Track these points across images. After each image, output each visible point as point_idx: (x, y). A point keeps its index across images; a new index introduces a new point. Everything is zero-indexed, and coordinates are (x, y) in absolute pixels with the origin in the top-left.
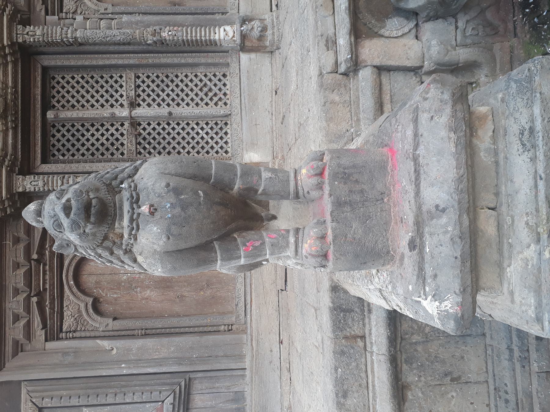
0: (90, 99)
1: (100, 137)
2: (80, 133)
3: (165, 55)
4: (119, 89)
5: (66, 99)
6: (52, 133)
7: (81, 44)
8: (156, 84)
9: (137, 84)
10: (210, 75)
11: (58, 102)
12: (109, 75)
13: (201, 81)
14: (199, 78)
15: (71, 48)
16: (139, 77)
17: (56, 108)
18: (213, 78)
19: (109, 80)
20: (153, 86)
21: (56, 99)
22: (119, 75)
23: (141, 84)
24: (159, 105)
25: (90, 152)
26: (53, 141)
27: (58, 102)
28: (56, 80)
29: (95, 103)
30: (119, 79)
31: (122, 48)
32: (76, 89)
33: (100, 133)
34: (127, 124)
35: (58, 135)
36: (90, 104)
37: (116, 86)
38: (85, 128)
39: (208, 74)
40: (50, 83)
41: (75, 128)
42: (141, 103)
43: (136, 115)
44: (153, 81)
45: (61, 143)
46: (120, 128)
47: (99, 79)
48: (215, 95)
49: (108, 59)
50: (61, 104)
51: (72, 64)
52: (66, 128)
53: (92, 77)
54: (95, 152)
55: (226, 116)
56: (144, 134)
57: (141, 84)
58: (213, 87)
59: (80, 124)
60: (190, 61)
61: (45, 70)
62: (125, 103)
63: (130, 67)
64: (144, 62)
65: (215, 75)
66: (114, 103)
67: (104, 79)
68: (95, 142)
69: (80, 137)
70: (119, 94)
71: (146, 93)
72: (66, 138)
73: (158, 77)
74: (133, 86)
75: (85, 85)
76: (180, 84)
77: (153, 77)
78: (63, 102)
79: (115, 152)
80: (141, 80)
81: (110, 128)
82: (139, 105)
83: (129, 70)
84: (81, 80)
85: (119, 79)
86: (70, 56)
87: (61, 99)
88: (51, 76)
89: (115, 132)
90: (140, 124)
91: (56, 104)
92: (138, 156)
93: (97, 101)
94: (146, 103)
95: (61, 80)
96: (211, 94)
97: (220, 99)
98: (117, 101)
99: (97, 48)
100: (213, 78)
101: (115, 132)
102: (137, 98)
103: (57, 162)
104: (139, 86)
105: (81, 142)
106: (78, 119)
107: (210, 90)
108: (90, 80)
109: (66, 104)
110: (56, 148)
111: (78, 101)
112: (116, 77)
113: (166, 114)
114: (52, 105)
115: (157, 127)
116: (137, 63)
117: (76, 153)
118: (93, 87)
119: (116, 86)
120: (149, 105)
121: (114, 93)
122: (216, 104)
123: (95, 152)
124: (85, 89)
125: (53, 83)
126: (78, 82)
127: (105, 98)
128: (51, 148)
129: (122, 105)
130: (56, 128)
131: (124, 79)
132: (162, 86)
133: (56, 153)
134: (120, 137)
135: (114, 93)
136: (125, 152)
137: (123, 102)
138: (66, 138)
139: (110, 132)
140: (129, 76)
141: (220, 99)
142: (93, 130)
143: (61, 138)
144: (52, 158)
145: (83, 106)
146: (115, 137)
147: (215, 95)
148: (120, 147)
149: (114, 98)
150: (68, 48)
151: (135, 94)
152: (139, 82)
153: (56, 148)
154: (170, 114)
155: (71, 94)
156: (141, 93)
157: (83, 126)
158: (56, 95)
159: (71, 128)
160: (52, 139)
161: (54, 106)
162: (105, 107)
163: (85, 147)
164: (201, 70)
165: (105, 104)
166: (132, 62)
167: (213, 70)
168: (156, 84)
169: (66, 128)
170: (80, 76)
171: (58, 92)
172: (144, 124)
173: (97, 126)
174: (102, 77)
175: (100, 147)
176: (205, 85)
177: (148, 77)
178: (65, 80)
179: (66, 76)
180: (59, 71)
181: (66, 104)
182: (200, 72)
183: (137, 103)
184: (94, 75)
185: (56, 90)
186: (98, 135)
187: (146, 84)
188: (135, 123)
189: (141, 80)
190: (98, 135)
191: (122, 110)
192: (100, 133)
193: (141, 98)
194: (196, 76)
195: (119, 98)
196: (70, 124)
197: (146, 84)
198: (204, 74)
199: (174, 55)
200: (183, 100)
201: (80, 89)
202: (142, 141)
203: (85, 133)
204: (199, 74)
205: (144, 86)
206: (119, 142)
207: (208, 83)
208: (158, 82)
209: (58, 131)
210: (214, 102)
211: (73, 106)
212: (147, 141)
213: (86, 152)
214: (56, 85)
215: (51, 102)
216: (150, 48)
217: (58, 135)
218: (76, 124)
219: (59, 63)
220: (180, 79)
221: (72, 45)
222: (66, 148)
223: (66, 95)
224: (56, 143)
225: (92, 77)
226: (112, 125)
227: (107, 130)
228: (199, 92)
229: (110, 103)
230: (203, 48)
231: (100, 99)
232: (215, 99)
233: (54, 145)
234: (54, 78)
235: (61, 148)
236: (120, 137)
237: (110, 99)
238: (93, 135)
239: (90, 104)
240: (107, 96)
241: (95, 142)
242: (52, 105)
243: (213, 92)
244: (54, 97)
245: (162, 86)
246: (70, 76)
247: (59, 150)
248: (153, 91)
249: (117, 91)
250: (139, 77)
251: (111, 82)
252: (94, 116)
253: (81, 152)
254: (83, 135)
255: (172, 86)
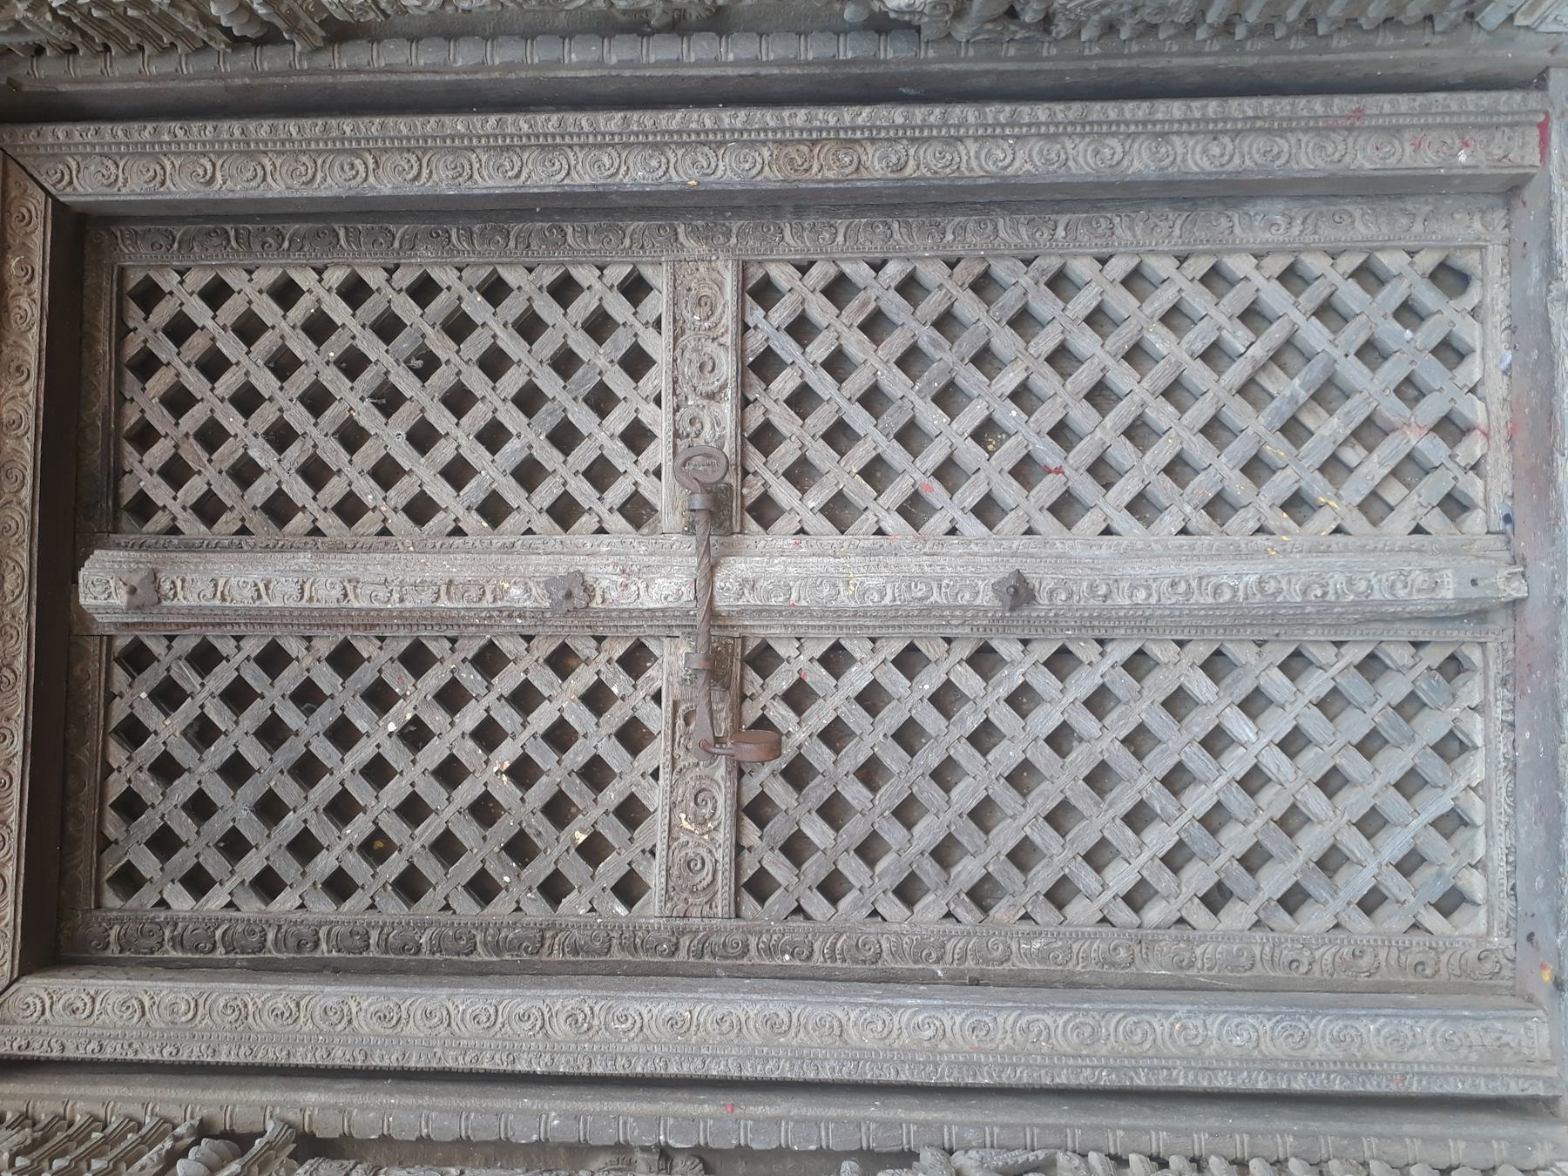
0: (404, 455)
1: (469, 753)
2: (325, 715)
3: (999, 112)
4: (618, 381)
5: (228, 453)
6: (119, 712)
7: (340, 33)
8: (896, 344)
9: (755, 344)
10: (1330, 275)
11: (175, 473)
12: (549, 276)
13: (1252, 316)
14: (1236, 300)
15: (270, 61)
16: (765, 293)
17: (160, 521)
18: (1351, 295)
19: (547, 309)
20: (874, 363)
21: (159, 453)
22: (618, 273)
23: (786, 347)
24: (914, 509)
25: (394, 866)
26: (128, 770)
27: (175, 473)
28: (163, 312)
29: (440, 491)
30: (619, 308)
31: (659, 57)
32: (301, 380)
33: (470, 717)
34: (673, 661)
35: (167, 730)
36: (403, 491)
37: (600, 361)
38: (364, 676)
39: (1314, 263)
40: (123, 331)
41: (290, 678)
42: (783, 493)
43: (750, 599)
44: (875, 326)
45: (183, 789)
46: (619, 684)
47: (476, 307)
48: (1369, 431)
49: (549, 146)
50: (194, 489)
51: (277, 188)
52: (222, 677)
53: (423, 291)
54: (430, 867)
55: (1469, 616)
56: (800, 736)
57: (786, 347)
58: (1353, 371)
59: (324, 647)
60: (1197, 158)
61: (81, 234)
62: (662, 494)
63: (709, 209)
64: (826, 169)
65: (1369, 276)
66: (582, 491)
67: (513, 307)
68: (432, 793)
69: (325, 751)
70: (618, 420)
71: (821, 419)
72: (219, 752)
73: (910, 287)
74: (727, 367)
75: (371, 346)
76: (1085, 342)
77: (878, 290)
78: (209, 475)
79: (575, 869)
80: (782, 313)
81: (544, 680)
82: (764, 511)
83: (694, 232)
84: (338, 310)
85: (619, 308)
86: (261, 129)
87: (193, 453)
88: (134, 278)
89: (580, 717)
90: (763, 659)
91: (159, 492)
92: (749, 904)
93: (457, 473)
94: (818, 496)
95: (198, 311)
96: (1329, 428)
97: (1410, 468)
98: (601, 474)
99: (464, 61)
100: (1351, 295)
101: (580, 717)
102: (756, 460)
103: (142, 955)
104: (765, 365)
105: (325, 789)
106: (310, 622)
107: (1328, 392)
108: (406, 308)
109: (226, 490)
110: (149, 823)
111: (315, 473)
112: (598, 290)
113: (986, 599)
114: (128, 494)
115: (894, 681)
116: (773, 177)
117: (287, 867)
118: (426, 365)
119: (600, 361)
120: (838, 511)
121: (582, 417)
122: (1374, 506)
123: (430, 867)
124: (368, 379)
125: (144, 331)
126: (319, 328)
127: (512, 452)
128: (113, 826)
129: (637, 511)
130: (152, 676)
131: (657, 303)
132: (947, 359)
133: (147, 863)
134: (615, 756)
135: (582, 417)
136: (654, 876)
137: (648, 488)
138: (219, 752)
139: (543, 718)
140: (695, 284)
141: (1410, 468)
142: (415, 697)
143: (184, 753)
144: (111, 899)
145: (350, 509)
146: (578, 756)
147: (1369, 431)
148: (613, 831)
149: (583, 456)
150: (244, 60)
151: (741, 423)
152: (769, 327)
153: (149, 823)
154: (1019, 593)
155: (265, 416)
156: (784, 420)
157: (344, 659)
158: (159, 418)
159: (255, 677)
160: (117, 754)
161: (144, 507)
162: (510, 523)
163: (358, 829)
164: (1262, 236)
165: (512, 493)
166: (728, 170)
167: (1362, 226)
168: (896, 344)
169: (222, 677)
170: (336, 276)
171: (179, 401)
172: (798, 662)
173: (448, 666)
174: (495, 291)
175: (467, 832)
176: (1287, 353)
177: (838, 290)
178: (232, 309)
179: (234, 278)
180: (186, 244)
181: (226, 490)
182: (1252, 245)
183: (753, 493)
184: (437, 274)
185: (159, 383)
186: (452, 735)
187: (820, 349)
188: (736, 658)
189: (782, 313)
190: (452, 735)
191: (636, 544)
192: (470, 717)
193: (785, 454)
194: (1215, 279)
195: (619, 455)
196: (253, 647)
197: (820, 349)
198: (1278, 264)
199: (1075, 110)
200: (1102, 471)
201: (334, 380)
202: (780, 793)
203: (362, 718)
204: (1239, 265)
205: (802, 365)
206: (612, 796)
207: (1315, 334)
208: (911, 326)
209: (168, 696)
210: (1356, 489)
211: (279, 509)
212: (818, 791)
213: (358, 868)
214: (164, 349)
215: (118, 473)
216: (892, 53)
217: (167, 730)
218: (293, 647)
219: (183, 188)
220: (1083, 303)
221: (269, 37)
222: (217, 826)
223: (231, 420)
224: (148, 788)
225: (423, 291)
226: (562, 661)
227: (525, 699)
228: (1238, 412)
229: (547, 493)
230: (1342, 53)
231: (477, 455)
232: (1372, 467)
233: (131, 806)
234: (149, 295)
235: (183, 826)
236: (615, 756)
237: (549, 456)
238: (415, 735)
239: (403, 491)
240: (527, 437)
241: (432, 793)
242: (128, 494)
243: (1353, 412)
244: (145, 436)
245: (947, 359)
246: (266, 277)
247: (164, 843)
248: (872, 399)
249: (602, 401)
250: (765, 293)
251: (564, 327)
252: (424, 599)
253: (324, 864)
254: (343, 734)
255: (1022, 360)
